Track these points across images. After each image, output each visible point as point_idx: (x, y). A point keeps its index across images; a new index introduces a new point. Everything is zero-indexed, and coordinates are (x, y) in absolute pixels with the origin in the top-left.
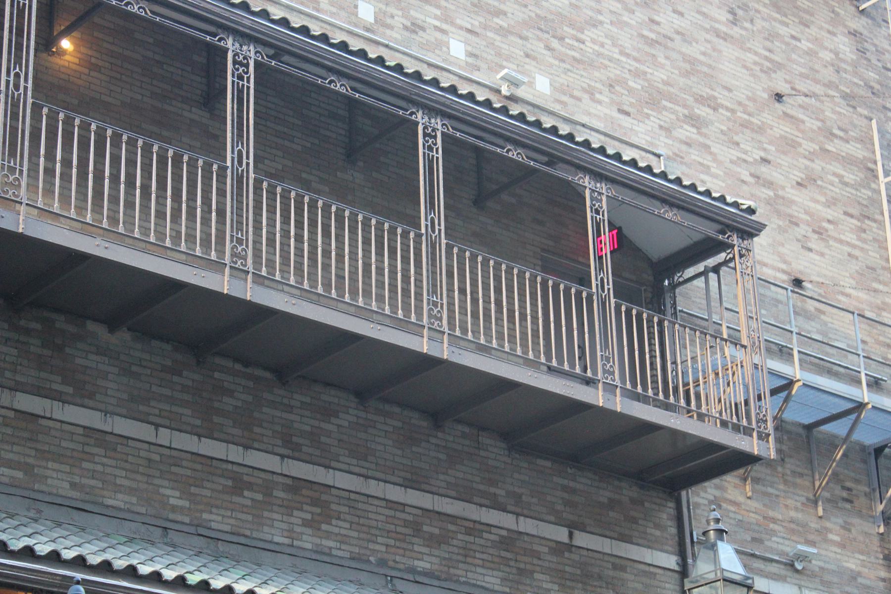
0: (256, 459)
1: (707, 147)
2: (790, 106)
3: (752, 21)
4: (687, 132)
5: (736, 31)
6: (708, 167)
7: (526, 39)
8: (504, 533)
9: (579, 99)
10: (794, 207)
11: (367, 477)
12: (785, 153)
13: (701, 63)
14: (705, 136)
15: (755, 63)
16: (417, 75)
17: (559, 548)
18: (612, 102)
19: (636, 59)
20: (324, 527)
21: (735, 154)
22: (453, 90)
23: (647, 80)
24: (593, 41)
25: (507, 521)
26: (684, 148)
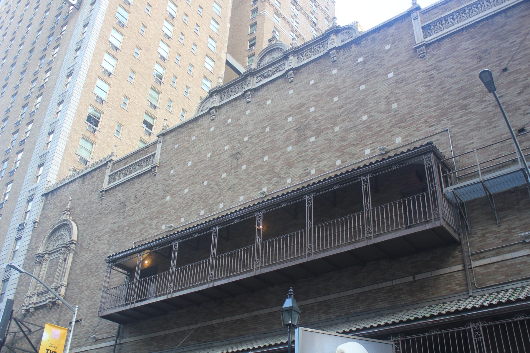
0: (309, 302)
1: (471, 112)
2: (511, 70)
3: (489, 54)
4: (462, 112)
5: (481, 63)
6: (471, 118)
7: (392, 131)
8: (389, 288)
9: (413, 135)
10: (517, 104)
11: (340, 292)
12: (510, 87)
13: (465, 86)
14: (469, 109)
15: (492, 66)
16: (206, 222)
17: (411, 283)
18: (426, 126)
19: (435, 106)
20: (329, 311)
21: (483, 106)
22: (190, 228)
23: (441, 109)
24: (418, 113)
25: (389, 283)
26: (459, 120)
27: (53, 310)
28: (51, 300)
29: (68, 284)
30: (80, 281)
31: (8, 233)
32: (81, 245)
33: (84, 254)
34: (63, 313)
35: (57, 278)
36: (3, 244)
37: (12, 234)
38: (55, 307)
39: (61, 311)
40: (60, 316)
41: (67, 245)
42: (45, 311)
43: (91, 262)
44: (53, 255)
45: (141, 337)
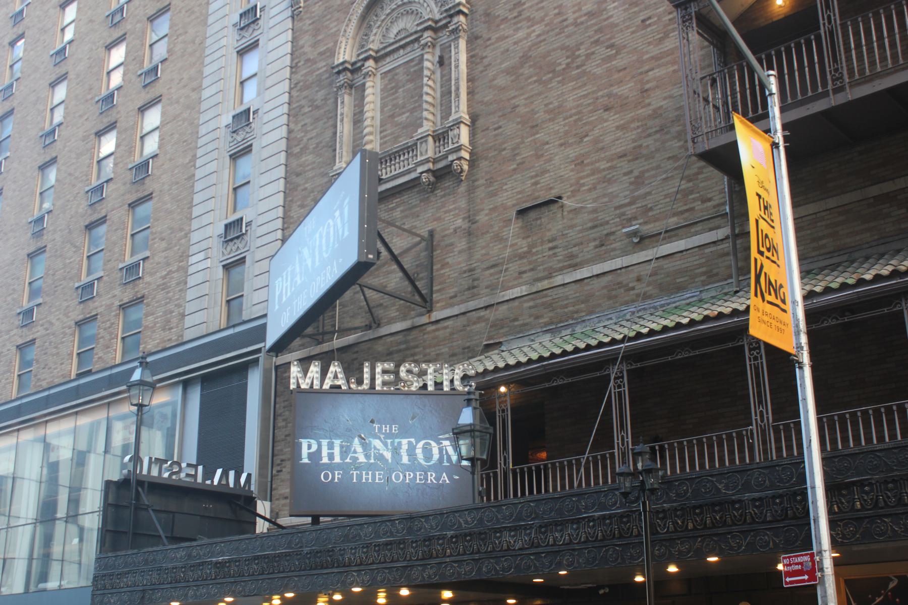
27: (439, 192)
28: (430, 166)
29: (474, 118)
30: (520, 101)
31: (209, 42)
32: (487, 15)
33: (507, 32)
34: (481, 193)
35: (431, 109)
36: (201, 72)
37: (224, 42)
38: (448, 183)
39: (471, 190)
40: (470, 201)
41: (436, 22)
42: (412, 198)
43: (542, 49)
44: (388, 59)
45: (832, 203)
